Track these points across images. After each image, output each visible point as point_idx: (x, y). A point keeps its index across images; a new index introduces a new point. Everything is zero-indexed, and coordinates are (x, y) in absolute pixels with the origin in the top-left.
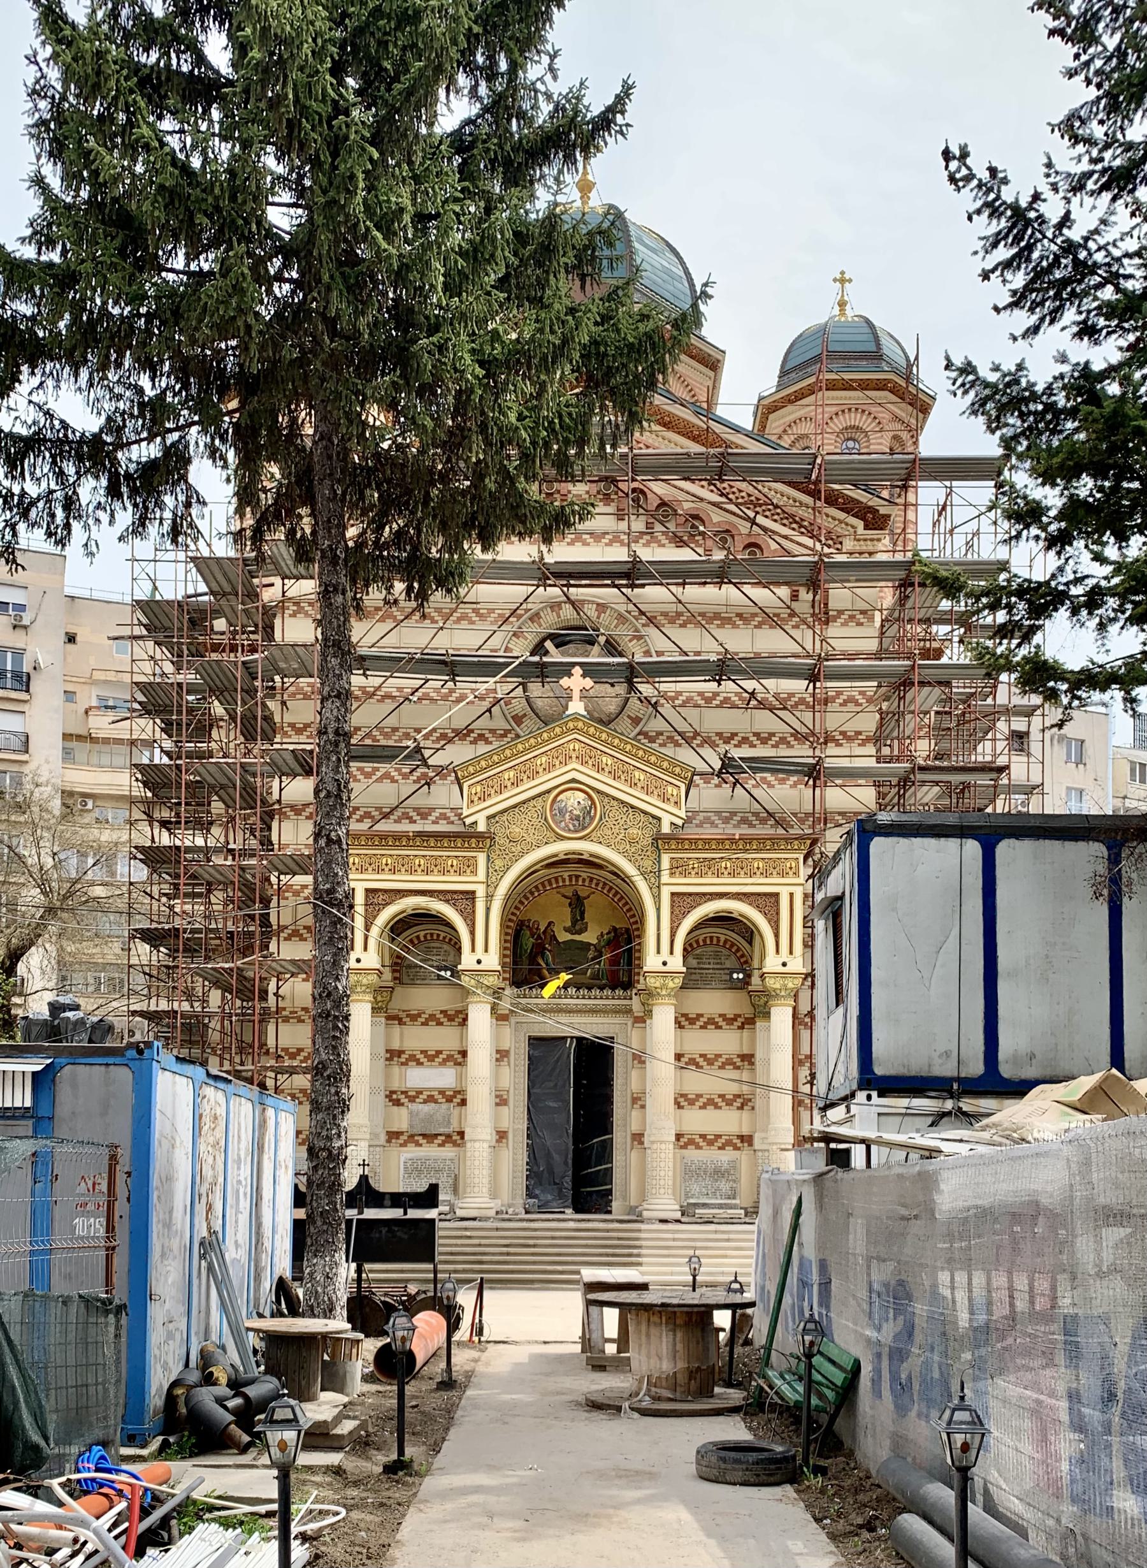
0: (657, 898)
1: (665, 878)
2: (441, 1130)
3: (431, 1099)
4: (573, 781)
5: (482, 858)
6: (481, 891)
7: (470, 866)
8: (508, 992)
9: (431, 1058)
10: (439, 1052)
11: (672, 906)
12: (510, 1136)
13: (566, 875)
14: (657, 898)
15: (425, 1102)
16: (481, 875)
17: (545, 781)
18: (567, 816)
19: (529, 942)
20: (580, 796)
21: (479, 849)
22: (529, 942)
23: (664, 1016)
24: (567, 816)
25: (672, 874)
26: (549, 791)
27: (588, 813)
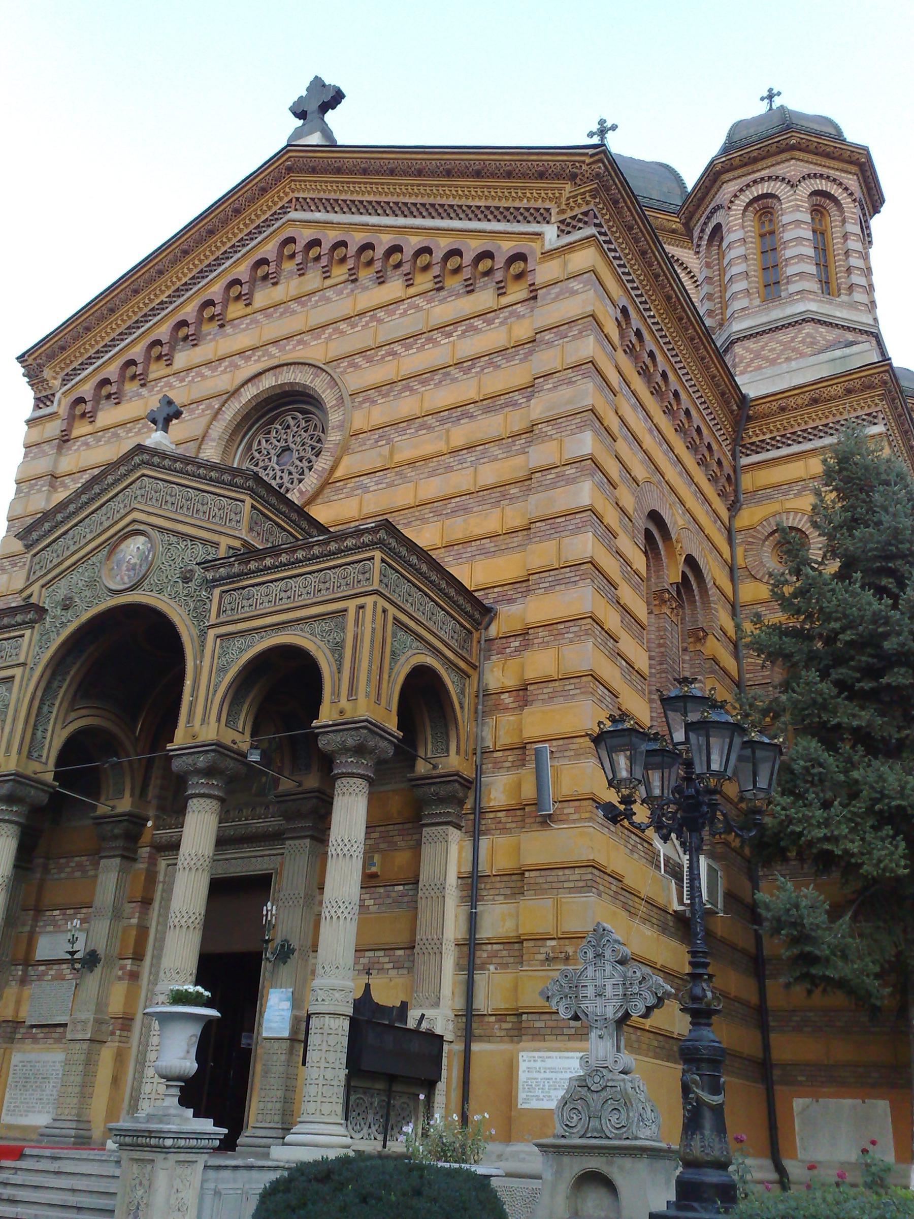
4: (134, 521)
24: (124, 568)
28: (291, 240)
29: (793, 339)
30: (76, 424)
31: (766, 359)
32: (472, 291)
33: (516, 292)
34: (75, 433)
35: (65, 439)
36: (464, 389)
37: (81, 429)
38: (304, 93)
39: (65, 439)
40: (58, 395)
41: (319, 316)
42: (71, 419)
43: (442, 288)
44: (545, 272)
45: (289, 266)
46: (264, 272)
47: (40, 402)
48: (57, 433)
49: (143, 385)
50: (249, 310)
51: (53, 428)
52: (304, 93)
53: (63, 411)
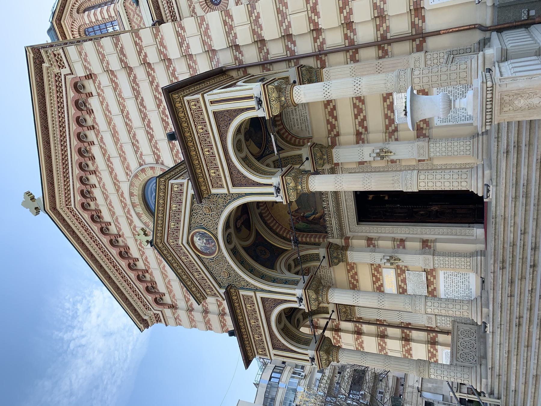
0: (240, 196)
1: (224, 191)
2: (424, 279)
3: (404, 281)
4: (188, 243)
5: (242, 292)
6: (259, 295)
7: (247, 298)
8: (331, 240)
9: (378, 279)
10: (373, 275)
11: (241, 185)
12: (425, 237)
13: (259, 211)
14: (240, 196)
15: (406, 284)
16: (251, 294)
17: (193, 257)
18: (208, 246)
19: (301, 225)
20: (196, 239)
21: (238, 295)
22: (301, 225)
23: (319, 184)
24: (208, 246)
25: (222, 186)
26: (198, 256)
27: (203, 235)
28: (83, 205)
29: (132, 10)
30: (165, 302)
31: (140, 21)
32: (92, 110)
33: (90, 86)
34: (170, 303)
35: (173, 307)
36: (131, 106)
37: (167, 299)
38: (28, 209)
39: (173, 307)
40: (155, 312)
41: (110, 188)
42: (163, 304)
43: (93, 126)
44: (80, 72)
45: (93, 206)
46: (96, 218)
47: (158, 320)
48: (169, 310)
49: (147, 272)
50: (112, 224)
51: (168, 312)
52: (28, 209)
53: (160, 308)
